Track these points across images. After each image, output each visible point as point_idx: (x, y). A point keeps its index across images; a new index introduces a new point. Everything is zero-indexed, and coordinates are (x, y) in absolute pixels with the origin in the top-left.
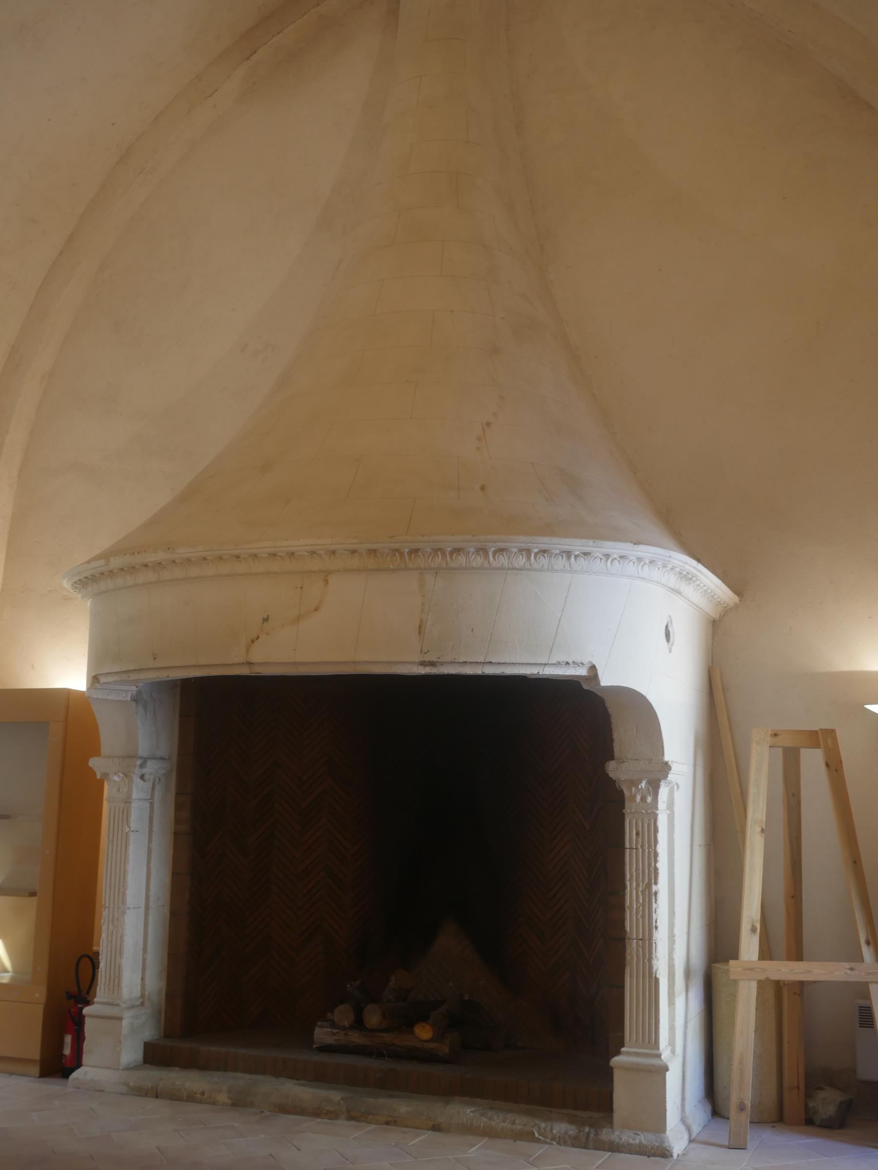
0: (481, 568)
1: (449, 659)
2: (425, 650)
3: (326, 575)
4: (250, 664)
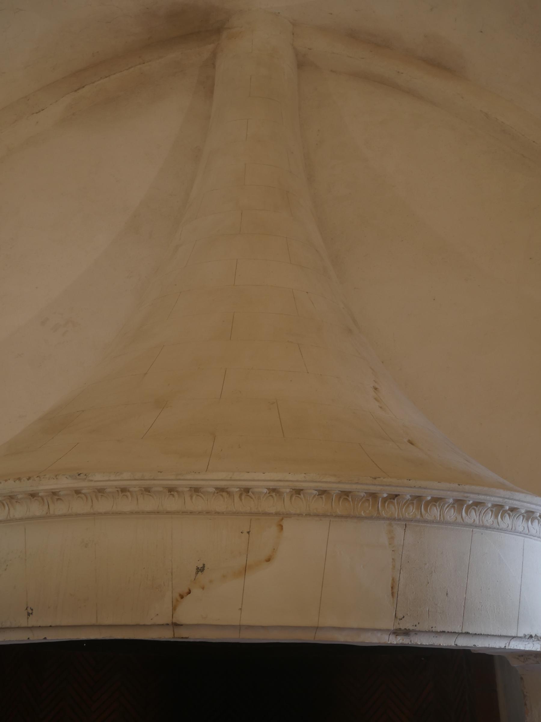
0: (455, 523)
1: (426, 627)
2: (400, 616)
3: (281, 518)
4: (176, 625)
